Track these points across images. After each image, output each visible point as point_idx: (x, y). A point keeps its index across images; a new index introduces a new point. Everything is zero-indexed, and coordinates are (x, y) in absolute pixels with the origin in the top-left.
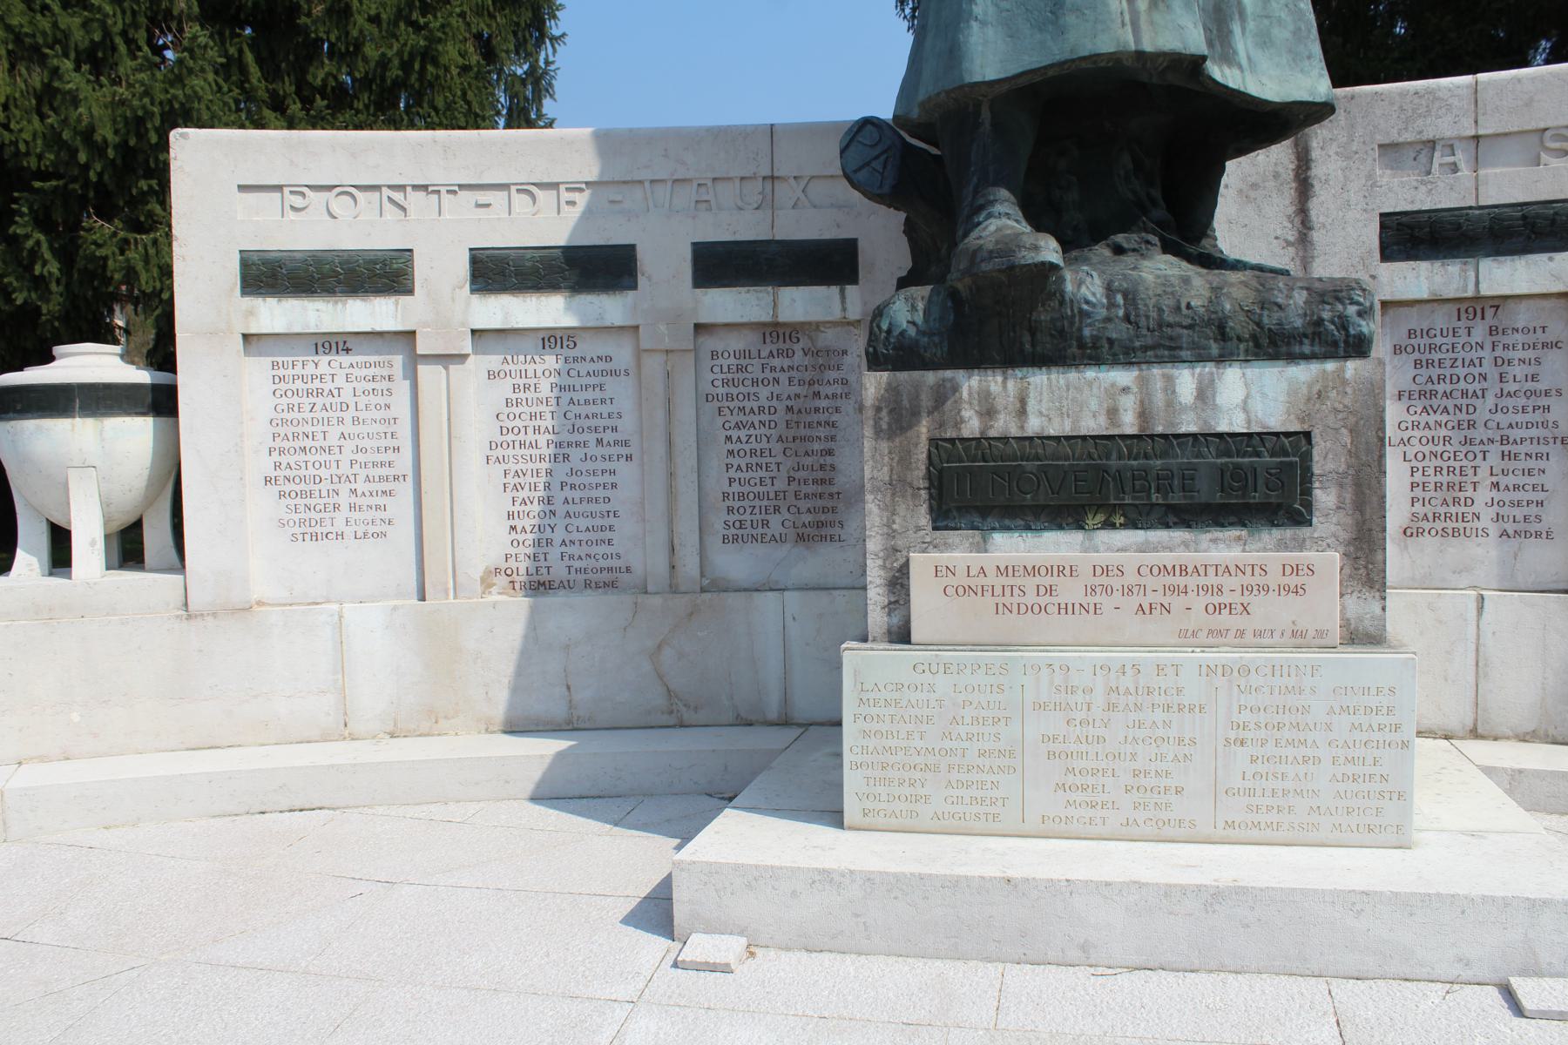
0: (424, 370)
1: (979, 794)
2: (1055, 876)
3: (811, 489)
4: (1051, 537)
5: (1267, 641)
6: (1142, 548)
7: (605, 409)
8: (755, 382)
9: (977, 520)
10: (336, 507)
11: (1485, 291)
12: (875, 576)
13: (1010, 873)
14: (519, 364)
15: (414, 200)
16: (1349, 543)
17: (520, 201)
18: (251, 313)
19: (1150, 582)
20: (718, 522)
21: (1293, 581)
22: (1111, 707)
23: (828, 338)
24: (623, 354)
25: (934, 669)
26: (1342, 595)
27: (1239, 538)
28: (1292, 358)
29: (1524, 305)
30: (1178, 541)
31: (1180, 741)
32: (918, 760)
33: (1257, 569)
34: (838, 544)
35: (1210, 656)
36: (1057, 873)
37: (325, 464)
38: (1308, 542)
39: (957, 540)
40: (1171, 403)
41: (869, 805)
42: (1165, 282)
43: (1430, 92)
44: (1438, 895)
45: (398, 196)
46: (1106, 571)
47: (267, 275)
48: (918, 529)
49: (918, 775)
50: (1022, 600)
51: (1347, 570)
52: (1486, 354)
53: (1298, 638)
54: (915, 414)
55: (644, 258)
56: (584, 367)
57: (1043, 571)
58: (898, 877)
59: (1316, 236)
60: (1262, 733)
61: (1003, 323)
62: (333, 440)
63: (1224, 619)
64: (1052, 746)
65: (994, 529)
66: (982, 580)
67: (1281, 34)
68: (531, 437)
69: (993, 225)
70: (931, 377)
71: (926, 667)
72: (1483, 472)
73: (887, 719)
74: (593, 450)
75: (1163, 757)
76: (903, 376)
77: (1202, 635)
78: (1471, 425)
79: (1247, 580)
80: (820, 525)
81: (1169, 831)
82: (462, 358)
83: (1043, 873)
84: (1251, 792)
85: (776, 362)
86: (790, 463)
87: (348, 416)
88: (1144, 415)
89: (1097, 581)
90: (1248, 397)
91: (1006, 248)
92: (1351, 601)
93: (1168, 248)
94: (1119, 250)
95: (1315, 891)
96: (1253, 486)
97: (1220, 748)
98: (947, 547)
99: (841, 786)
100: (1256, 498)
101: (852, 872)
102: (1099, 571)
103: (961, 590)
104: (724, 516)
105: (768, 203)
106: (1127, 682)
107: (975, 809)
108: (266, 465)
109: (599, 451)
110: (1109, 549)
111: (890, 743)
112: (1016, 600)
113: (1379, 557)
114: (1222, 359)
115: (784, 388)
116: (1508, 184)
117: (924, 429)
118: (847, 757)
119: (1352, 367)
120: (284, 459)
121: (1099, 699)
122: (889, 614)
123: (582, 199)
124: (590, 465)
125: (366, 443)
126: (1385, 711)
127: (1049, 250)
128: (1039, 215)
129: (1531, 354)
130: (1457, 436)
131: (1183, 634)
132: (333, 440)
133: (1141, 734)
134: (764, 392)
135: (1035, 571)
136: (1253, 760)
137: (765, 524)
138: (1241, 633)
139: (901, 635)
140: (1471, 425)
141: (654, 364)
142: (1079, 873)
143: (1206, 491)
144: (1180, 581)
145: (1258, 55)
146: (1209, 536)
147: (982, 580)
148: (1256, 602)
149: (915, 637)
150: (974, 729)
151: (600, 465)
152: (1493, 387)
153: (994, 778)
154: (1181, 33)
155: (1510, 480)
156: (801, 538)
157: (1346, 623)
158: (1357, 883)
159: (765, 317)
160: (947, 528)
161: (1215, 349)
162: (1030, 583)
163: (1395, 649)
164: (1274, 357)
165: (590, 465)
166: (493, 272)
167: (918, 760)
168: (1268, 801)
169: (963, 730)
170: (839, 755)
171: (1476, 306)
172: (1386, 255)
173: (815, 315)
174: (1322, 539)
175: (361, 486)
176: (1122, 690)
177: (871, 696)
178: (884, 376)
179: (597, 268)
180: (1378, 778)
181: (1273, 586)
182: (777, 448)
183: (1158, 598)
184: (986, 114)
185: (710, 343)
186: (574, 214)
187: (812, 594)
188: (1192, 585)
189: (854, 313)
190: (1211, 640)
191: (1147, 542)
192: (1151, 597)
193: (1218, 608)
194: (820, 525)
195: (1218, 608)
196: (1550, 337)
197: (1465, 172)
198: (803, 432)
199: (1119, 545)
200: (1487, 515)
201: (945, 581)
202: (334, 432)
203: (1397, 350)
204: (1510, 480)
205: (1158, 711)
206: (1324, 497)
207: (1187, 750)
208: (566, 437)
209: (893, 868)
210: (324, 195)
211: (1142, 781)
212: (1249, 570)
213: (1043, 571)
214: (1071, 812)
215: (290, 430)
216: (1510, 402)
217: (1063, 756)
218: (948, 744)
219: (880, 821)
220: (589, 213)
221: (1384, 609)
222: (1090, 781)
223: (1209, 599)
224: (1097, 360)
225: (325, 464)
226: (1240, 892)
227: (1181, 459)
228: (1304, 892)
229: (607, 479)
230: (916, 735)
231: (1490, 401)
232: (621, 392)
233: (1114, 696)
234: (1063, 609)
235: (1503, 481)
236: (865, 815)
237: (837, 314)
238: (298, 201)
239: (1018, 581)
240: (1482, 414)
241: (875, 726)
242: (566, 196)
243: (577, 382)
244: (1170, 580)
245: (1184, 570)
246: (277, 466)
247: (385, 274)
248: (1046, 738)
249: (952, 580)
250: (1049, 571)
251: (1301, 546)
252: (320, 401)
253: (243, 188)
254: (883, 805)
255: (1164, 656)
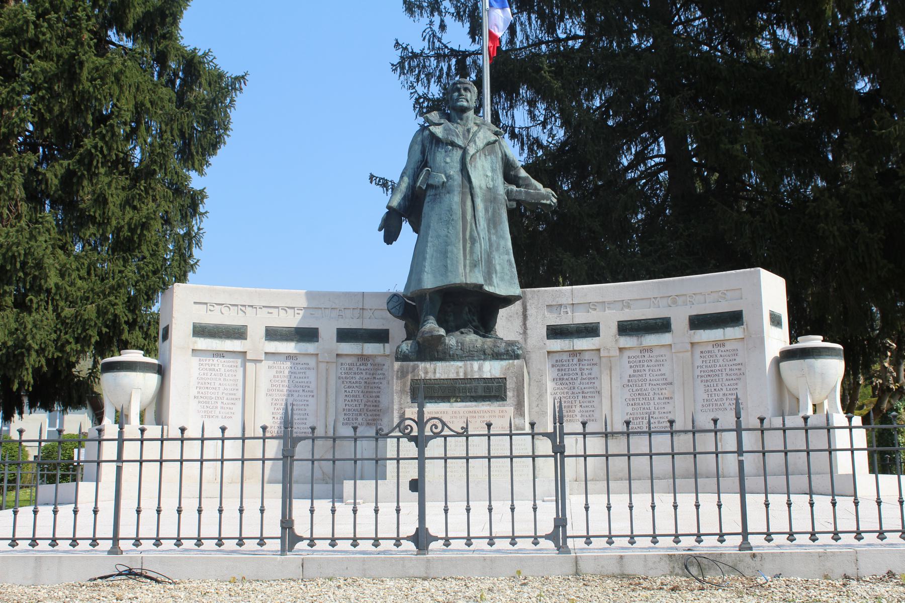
0: (248, 364)
3: (372, 408)
7: (306, 380)
8: (355, 373)
10: (216, 407)
11: (576, 348)
14: (279, 364)
15: (249, 310)
17: (282, 312)
18: (195, 342)
20: (341, 418)
21: (501, 414)
22: (456, 446)
23: (379, 360)
24: (312, 362)
28: (502, 359)
29: (587, 353)
37: (214, 393)
40: (472, 371)
42: (471, 340)
43: (560, 290)
45: (243, 308)
47: (200, 331)
52: (577, 367)
54: (407, 373)
55: (322, 333)
56: (300, 366)
59: (528, 332)
61: (429, 350)
62: (217, 385)
67: (507, 277)
68: (281, 388)
69: (428, 325)
70: (412, 363)
72: (577, 402)
74: (301, 393)
76: (405, 363)
78: (574, 388)
82: (261, 361)
85: (362, 367)
86: (365, 399)
87: (222, 378)
88: (465, 373)
90: (491, 369)
91: (431, 331)
92: (517, 420)
93: (476, 333)
94: (462, 333)
96: (493, 391)
100: (493, 394)
104: (343, 416)
105: (361, 317)
108: (194, 392)
109: (304, 394)
114: (484, 360)
115: (364, 376)
116: (581, 318)
117: (410, 377)
119: (516, 361)
120: (201, 391)
123: (301, 312)
124: (300, 398)
125: (228, 387)
127: (442, 332)
128: (441, 323)
129: (589, 367)
130: (570, 392)
132: (217, 385)
134: (358, 377)
137: (357, 419)
140: (574, 388)
141: (323, 366)
143: (480, 392)
145: (500, 283)
151: (303, 398)
152: (580, 377)
154: (476, 278)
155: (585, 404)
156: (368, 424)
159: (359, 353)
161: (483, 357)
164: (497, 359)
165: (300, 398)
166: (272, 334)
171: (574, 353)
172: (548, 338)
173: (375, 352)
175: (225, 401)
178: (399, 363)
179: (306, 335)
182: (361, 395)
184: (428, 296)
185: (341, 360)
186: (300, 317)
189: (388, 352)
194: (374, 420)
196: (594, 362)
197: (570, 313)
198: (370, 390)
200: (579, 415)
202: (218, 383)
203: (553, 366)
204: (585, 404)
206: (509, 394)
208: (293, 389)
210: (220, 307)
215: (203, 381)
216: (584, 381)
220: (304, 317)
224: (454, 360)
225: (214, 393)
227: (474, 384)
229: (305, 403)
231: (579, 381)
232: (312, 375)
235: (583, 405)
237: (382, 352)
238: (212, 308)
240: (576, 386)
242: (297, 311)
243: (297, 371)
246: (198, 393)
247: (238, 333)
252: (213, 373)
253: (195, 303)
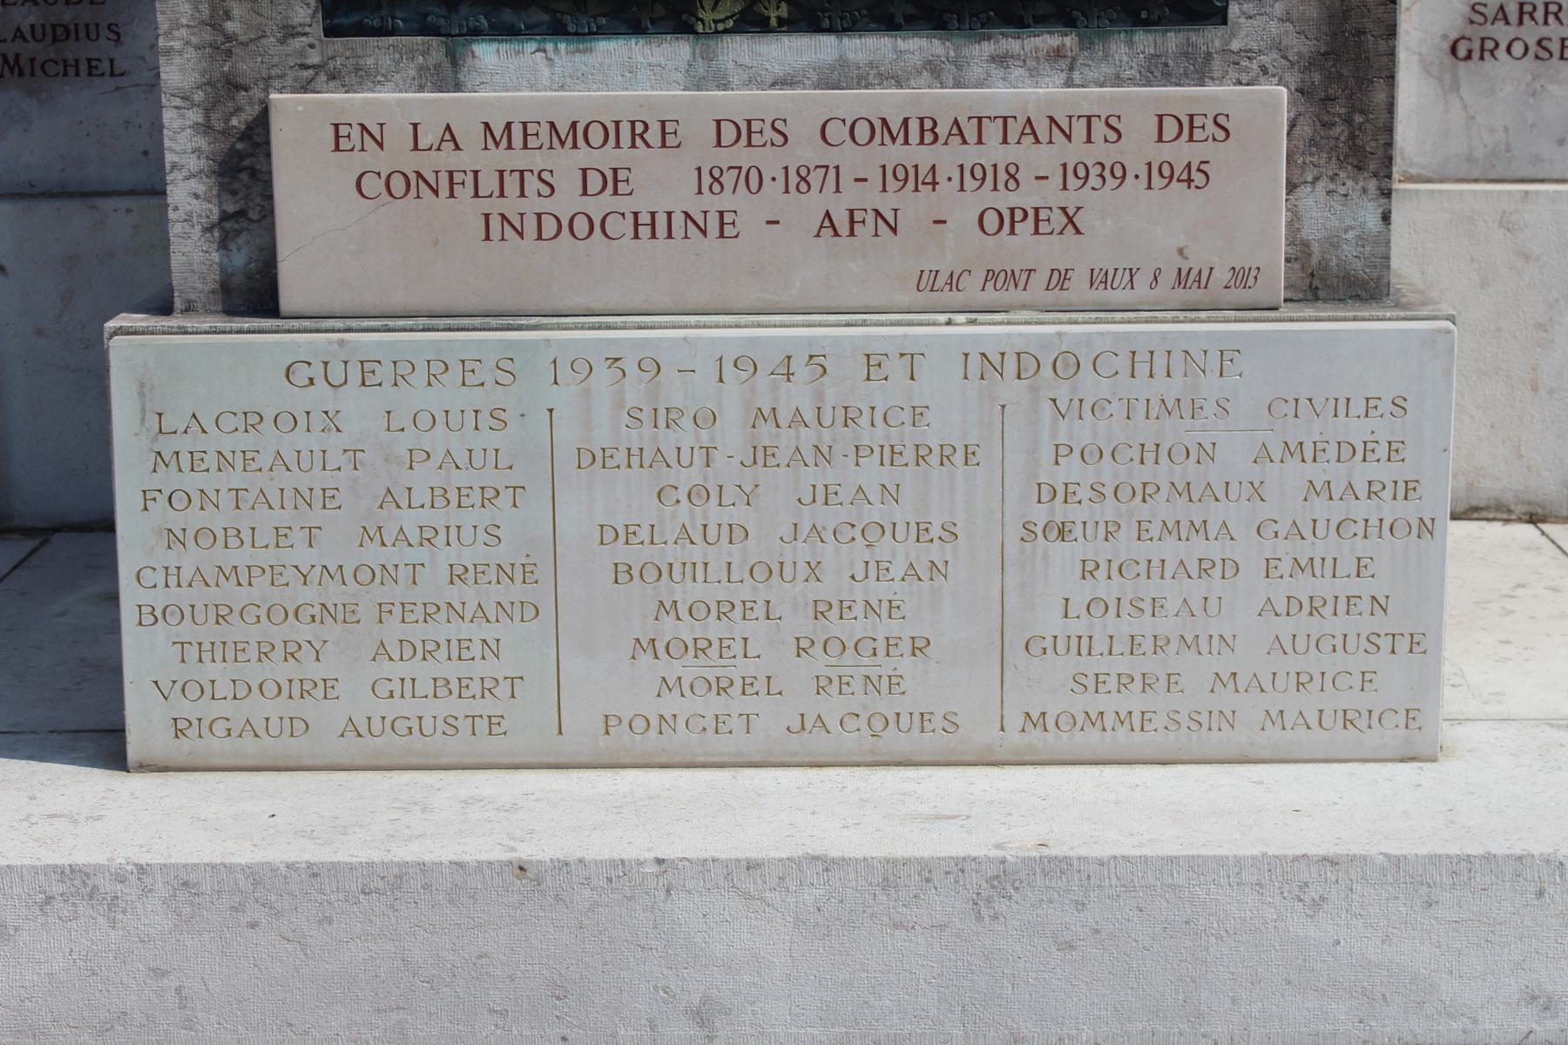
1: (452, 670)
2: (629, 853)
4: (612, 51)
5: (1120, 296)
6: (832, 78)
9: (435, 16)
12: (184, 147)
13: (525, 852)
16: (1310, 65)
19: (850, 159)
21: (1181, 153)
22: (761, 456)
25: (336, 375)
26: (1292, 187)
27: (1058, 54)
30: (916, 60)
31: (921, 531)
32: (308, 594)
33: (1099, 128)
34: (111, 83)
35: (992, 331)
36: (634, 843)
38: (1217, 64)
39: (386, 61)
41: (187, 709)
44: (1488, 858)
46: (746, 132)
48: (290, 32)
49: (304, 632)
50: (546, 205)
51: (1305, 129)
53: (1192, 289)
57: (596, 135)
58: (257, 875)
60: (1108, 510)
63: (1023, 246)
64: (622, 553)
65: (476, 33)
66: (448, 159)
71: (317, 371)
73: (226, 499)
75: (881, 570)
77: (972, 288)
79: (1076, 152)
80: (61, 33)
81: (895, 741)
83: (601, 846)
84: (1081, 645)
89: (726, 158)
95: (1221, 861)
97: (1012, 547)
98: (361, 77)
99: (117, 670)
101: (142, 869)
102: (728, 133)
103: (398, 184)
106: (797, 396)
107: (443, 707)
110: (751, 82)
111: (239, 557)
112: (532, 204)
113: (1380, 97)
118: (130, 595)
121: (731, 436)
122: (223, 245)
126: (1382, 451)
131: (927, 281)
133: (828, 517)
135: (575, 135)
136: (1088, 571)
138: (1061, 278)
139: (254, 295)
142: (685, 844)
144: (918, 155)
146: (988, 48)
147: (448, 159)
148: (1095, 203)
149: (289, 298)
150: (438, 518)
153: (489, 632)
157: (1299, 252)
158: (1315, 839)
160: (361, 31)
162: (566, 164)
163: (1406, 308)
167: (308, 594)
168: (1122, 664)
169: (410, 520)
170: (113, 598)
174: (1248, 54)
176: (784, 416)
177: (184, 444)
180: (1365, 605)
181: (1136, 166)
183: (870, 197)
187: (45, 208)
188: (947, 169)
190: (992, 296)
191: (842, 63)
192: (852, 195)
193: (1009, 220)
194: (61, 33)
195: (1009, 220)
199: (778, 70)
201: (358, 162)
205: (870, 463)
207: (936, 552)
209: (244, 854)
211: (836, 627)
212: (1079, 128)
213: (596, 135)
214: (671, 704)
217: (651, 574)
218: (374, 555)
219: (216, 746)
221: (1386, 218)
222: (715, 629)
223: (987, 197)
226: (1053, 869)
228: (1196, 865)
230: (298, 537)
233: (766, 429)
234: (645, 225)
236: (179, 733)
239: (537, 160)
241: (195, 518)
244: (896, 154)
245: (929, 131)
248: (607, 534)
249: (373, 159)
250: (611, 133)
251: (1201, 73)
254: (219, 708)
255: (882, 333)
